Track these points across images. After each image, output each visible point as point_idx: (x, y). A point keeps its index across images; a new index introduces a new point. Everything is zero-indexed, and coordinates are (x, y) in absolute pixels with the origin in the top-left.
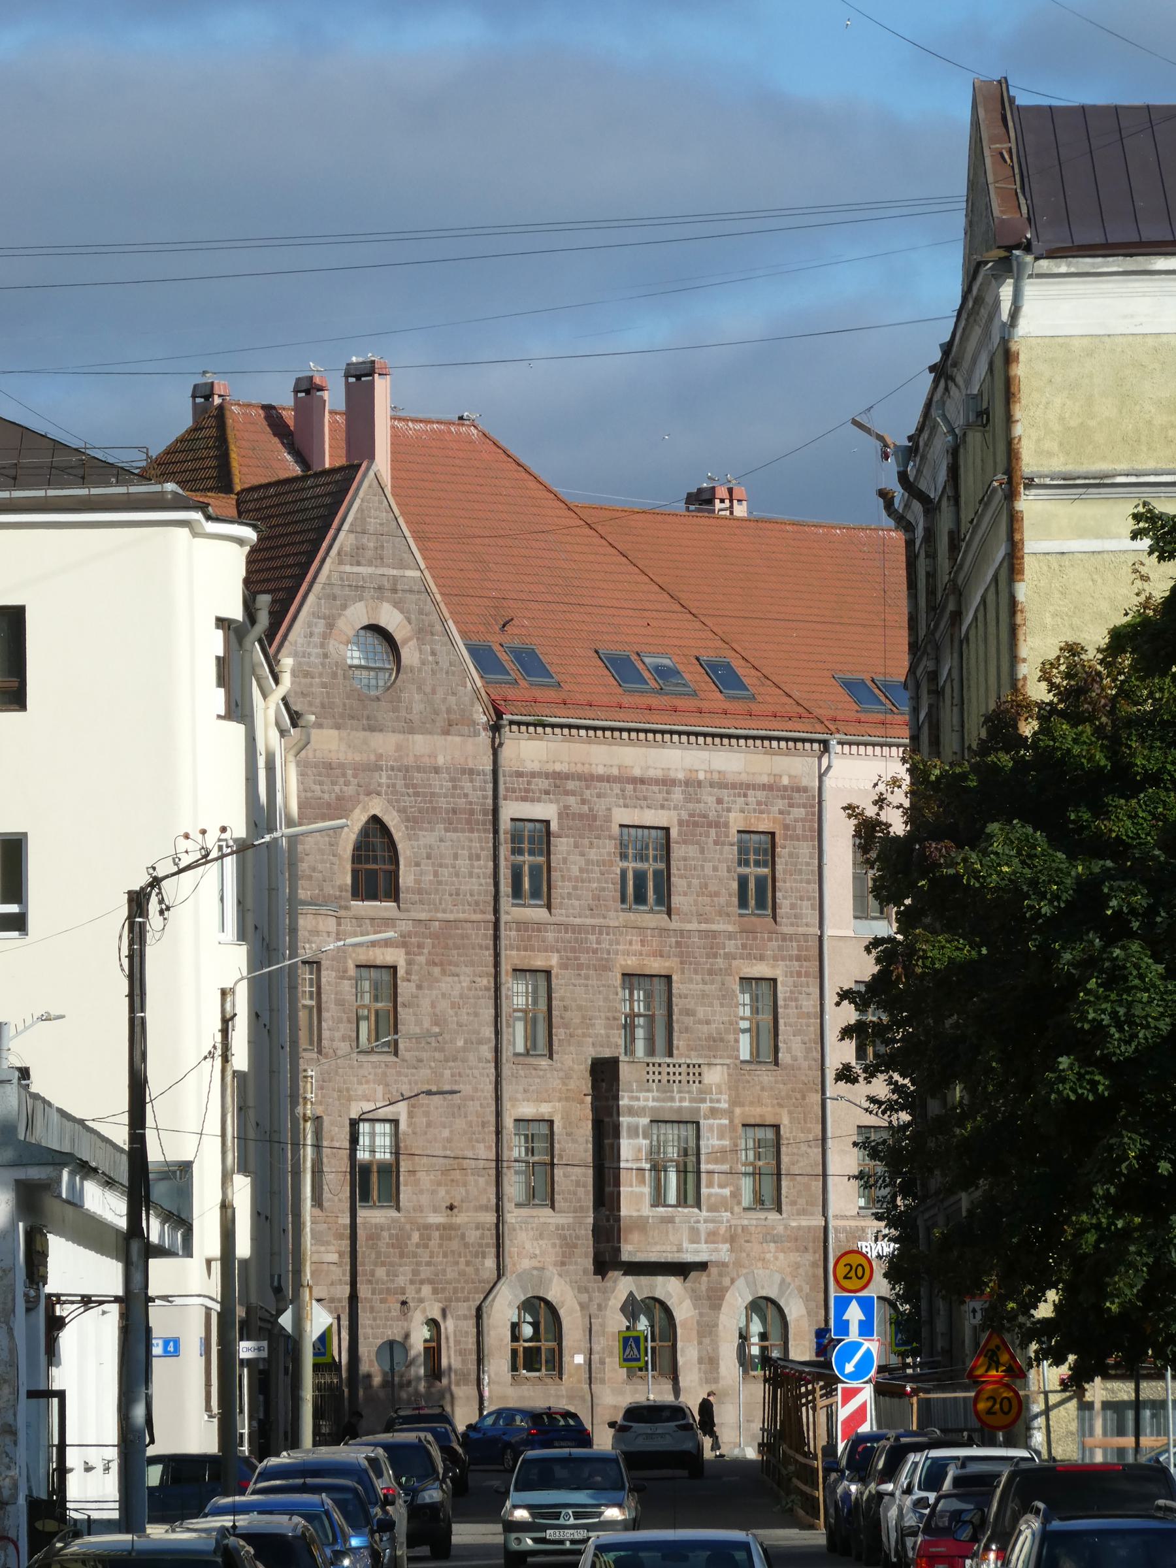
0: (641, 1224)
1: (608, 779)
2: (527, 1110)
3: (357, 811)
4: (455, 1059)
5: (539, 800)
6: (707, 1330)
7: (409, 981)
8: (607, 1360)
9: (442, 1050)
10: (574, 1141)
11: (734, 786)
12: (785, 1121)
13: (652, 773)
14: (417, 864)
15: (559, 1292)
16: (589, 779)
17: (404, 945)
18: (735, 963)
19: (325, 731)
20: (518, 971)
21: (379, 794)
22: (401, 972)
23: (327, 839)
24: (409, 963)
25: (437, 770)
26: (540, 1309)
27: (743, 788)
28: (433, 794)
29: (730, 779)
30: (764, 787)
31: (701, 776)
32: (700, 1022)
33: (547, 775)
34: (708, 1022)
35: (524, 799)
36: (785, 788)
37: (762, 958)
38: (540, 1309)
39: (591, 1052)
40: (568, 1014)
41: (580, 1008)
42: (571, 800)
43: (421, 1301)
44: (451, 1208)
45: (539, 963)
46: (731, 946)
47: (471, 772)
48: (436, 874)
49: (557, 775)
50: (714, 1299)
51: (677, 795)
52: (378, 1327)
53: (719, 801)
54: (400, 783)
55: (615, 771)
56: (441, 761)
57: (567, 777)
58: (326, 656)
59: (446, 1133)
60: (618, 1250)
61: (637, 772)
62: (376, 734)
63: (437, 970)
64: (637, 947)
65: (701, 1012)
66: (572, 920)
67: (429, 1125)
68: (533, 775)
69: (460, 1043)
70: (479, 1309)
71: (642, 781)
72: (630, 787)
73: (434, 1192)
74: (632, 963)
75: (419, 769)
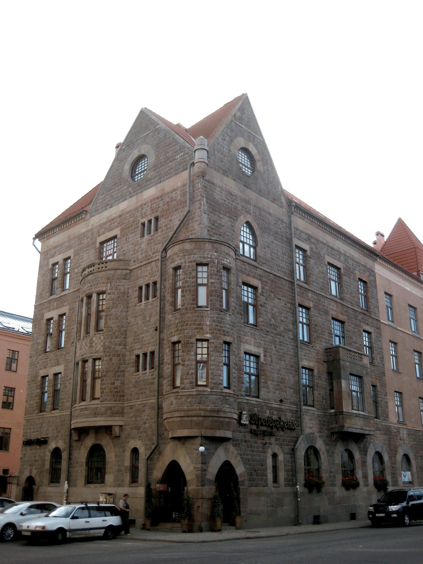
0: (350, 415)
1: (323, 243)
2: (305, 363)
3: (242, 217)
4: (280, 335)
5: (303, 242)
6: (364, 463)
7: (263, 295)
8: (336, 476)
9: (276, 330)
10: (321, 380)
11: (357, 262)
12: (378, 385)
13: (335, 247)
14: (265, 248)
15: (320, 445)
16: (318, 241)
17: (260, 280)
18: (362, 324)
19: (229, 179)
20: (300, 305)
21: (250, 214)
22: (260, 290)
23: (230, 223)
24: (263, 288)
25: (270, 214)
26: (313, 450)
27: (359, 264)
28: (269, 223)
29: (355, 259)
30: (363, 266)
31: (348, 255)
32: (353, 342)
33: (306, 234)
34: (356, 343)
35: (299, 239)
36: (368, 269)
37: (368, 324)
38: (313, 450)
39: (324, 345)
40: (317, 328)
41: (320, 326)
42: (313, 246)
43: (270, 444)
44: (281, 401)
45: (306, 304)
46: (360, 317)
47: (282, 221)
48: (271, 255)
49: (308, 235)
50: (364, 452)
51: (342, 258)
52: (254, 455)
53: (353, 266)
54: (257, 213)
55: (325, 242)
56: (271, 211)
57: (311, 237)
58: (230, 150)
59: (278, 367)
60: (343, 426)
61: (331, 245)
62: (249, 190)
63: (272, 295)
64: (335, 308)
65: (354, 338)
66: (315, 291)
67: (272, 362)
68: (301, 231)
69: (282, 328)
70: (293, 450)
71: (333, 249)
72: (329, 249)
73: (274, 393)
74: (333, 313)
75: (264, 211)
